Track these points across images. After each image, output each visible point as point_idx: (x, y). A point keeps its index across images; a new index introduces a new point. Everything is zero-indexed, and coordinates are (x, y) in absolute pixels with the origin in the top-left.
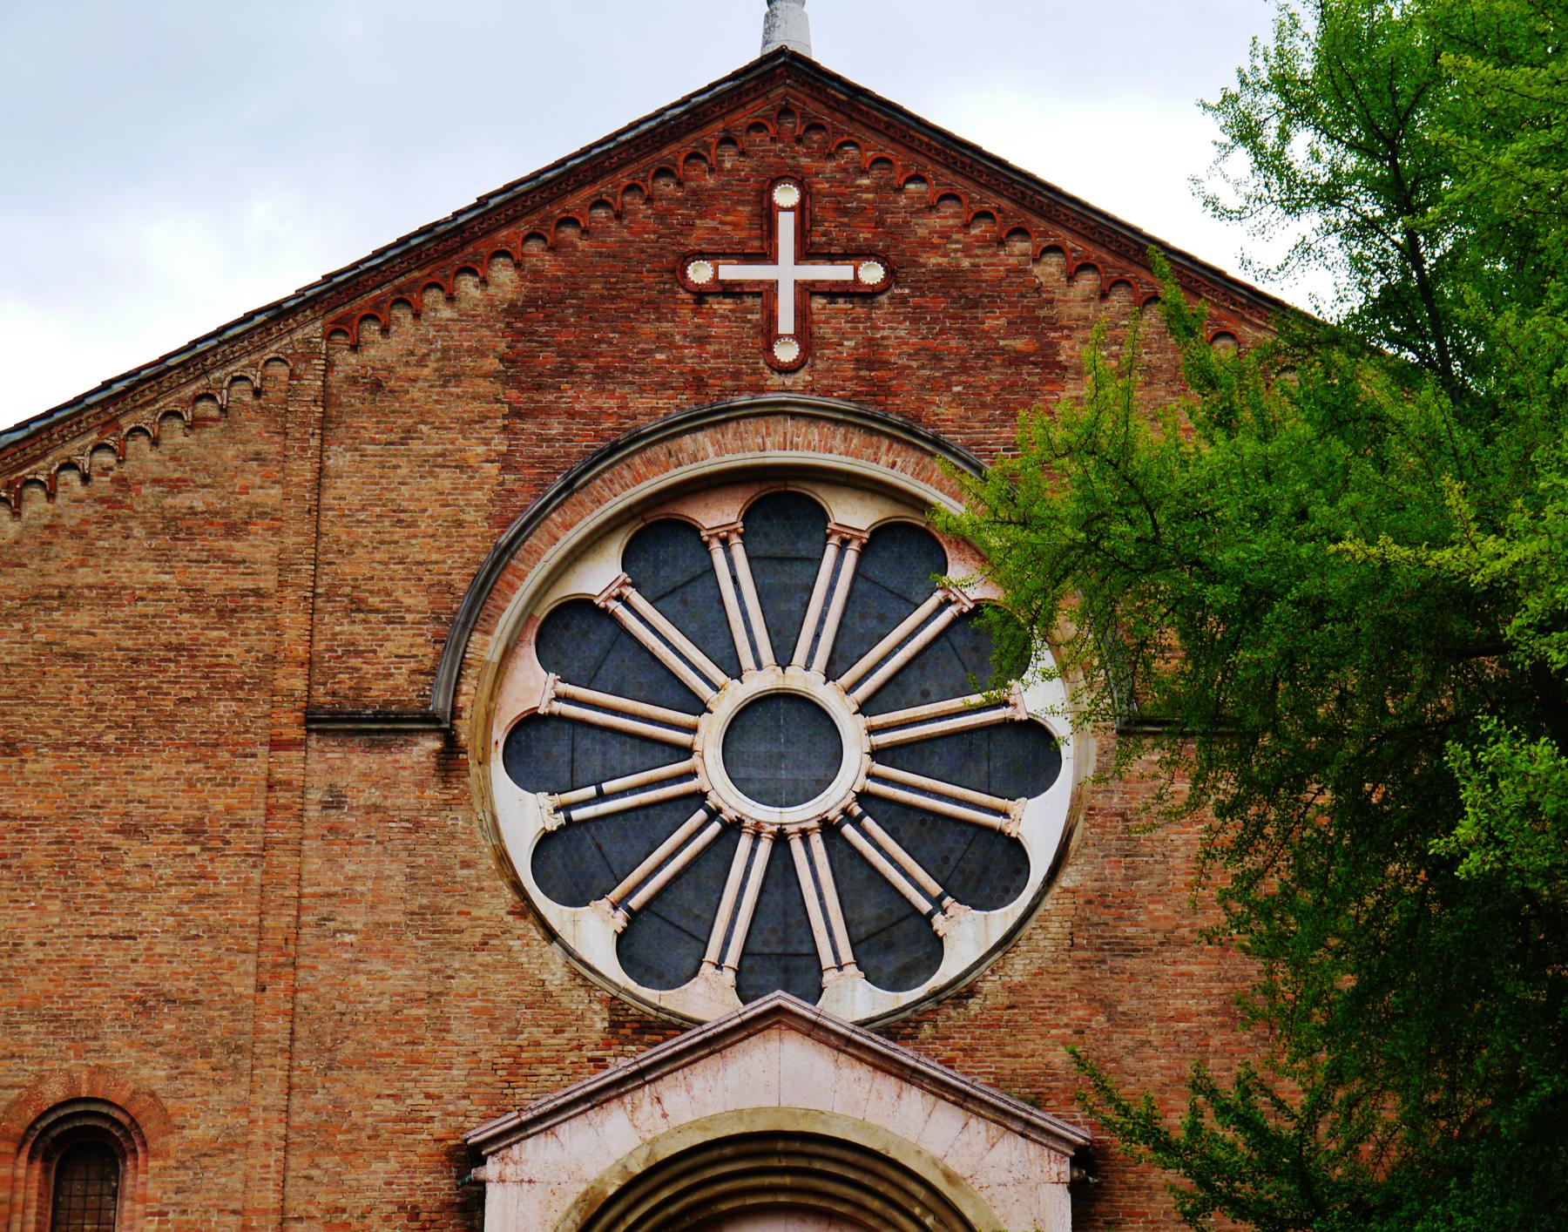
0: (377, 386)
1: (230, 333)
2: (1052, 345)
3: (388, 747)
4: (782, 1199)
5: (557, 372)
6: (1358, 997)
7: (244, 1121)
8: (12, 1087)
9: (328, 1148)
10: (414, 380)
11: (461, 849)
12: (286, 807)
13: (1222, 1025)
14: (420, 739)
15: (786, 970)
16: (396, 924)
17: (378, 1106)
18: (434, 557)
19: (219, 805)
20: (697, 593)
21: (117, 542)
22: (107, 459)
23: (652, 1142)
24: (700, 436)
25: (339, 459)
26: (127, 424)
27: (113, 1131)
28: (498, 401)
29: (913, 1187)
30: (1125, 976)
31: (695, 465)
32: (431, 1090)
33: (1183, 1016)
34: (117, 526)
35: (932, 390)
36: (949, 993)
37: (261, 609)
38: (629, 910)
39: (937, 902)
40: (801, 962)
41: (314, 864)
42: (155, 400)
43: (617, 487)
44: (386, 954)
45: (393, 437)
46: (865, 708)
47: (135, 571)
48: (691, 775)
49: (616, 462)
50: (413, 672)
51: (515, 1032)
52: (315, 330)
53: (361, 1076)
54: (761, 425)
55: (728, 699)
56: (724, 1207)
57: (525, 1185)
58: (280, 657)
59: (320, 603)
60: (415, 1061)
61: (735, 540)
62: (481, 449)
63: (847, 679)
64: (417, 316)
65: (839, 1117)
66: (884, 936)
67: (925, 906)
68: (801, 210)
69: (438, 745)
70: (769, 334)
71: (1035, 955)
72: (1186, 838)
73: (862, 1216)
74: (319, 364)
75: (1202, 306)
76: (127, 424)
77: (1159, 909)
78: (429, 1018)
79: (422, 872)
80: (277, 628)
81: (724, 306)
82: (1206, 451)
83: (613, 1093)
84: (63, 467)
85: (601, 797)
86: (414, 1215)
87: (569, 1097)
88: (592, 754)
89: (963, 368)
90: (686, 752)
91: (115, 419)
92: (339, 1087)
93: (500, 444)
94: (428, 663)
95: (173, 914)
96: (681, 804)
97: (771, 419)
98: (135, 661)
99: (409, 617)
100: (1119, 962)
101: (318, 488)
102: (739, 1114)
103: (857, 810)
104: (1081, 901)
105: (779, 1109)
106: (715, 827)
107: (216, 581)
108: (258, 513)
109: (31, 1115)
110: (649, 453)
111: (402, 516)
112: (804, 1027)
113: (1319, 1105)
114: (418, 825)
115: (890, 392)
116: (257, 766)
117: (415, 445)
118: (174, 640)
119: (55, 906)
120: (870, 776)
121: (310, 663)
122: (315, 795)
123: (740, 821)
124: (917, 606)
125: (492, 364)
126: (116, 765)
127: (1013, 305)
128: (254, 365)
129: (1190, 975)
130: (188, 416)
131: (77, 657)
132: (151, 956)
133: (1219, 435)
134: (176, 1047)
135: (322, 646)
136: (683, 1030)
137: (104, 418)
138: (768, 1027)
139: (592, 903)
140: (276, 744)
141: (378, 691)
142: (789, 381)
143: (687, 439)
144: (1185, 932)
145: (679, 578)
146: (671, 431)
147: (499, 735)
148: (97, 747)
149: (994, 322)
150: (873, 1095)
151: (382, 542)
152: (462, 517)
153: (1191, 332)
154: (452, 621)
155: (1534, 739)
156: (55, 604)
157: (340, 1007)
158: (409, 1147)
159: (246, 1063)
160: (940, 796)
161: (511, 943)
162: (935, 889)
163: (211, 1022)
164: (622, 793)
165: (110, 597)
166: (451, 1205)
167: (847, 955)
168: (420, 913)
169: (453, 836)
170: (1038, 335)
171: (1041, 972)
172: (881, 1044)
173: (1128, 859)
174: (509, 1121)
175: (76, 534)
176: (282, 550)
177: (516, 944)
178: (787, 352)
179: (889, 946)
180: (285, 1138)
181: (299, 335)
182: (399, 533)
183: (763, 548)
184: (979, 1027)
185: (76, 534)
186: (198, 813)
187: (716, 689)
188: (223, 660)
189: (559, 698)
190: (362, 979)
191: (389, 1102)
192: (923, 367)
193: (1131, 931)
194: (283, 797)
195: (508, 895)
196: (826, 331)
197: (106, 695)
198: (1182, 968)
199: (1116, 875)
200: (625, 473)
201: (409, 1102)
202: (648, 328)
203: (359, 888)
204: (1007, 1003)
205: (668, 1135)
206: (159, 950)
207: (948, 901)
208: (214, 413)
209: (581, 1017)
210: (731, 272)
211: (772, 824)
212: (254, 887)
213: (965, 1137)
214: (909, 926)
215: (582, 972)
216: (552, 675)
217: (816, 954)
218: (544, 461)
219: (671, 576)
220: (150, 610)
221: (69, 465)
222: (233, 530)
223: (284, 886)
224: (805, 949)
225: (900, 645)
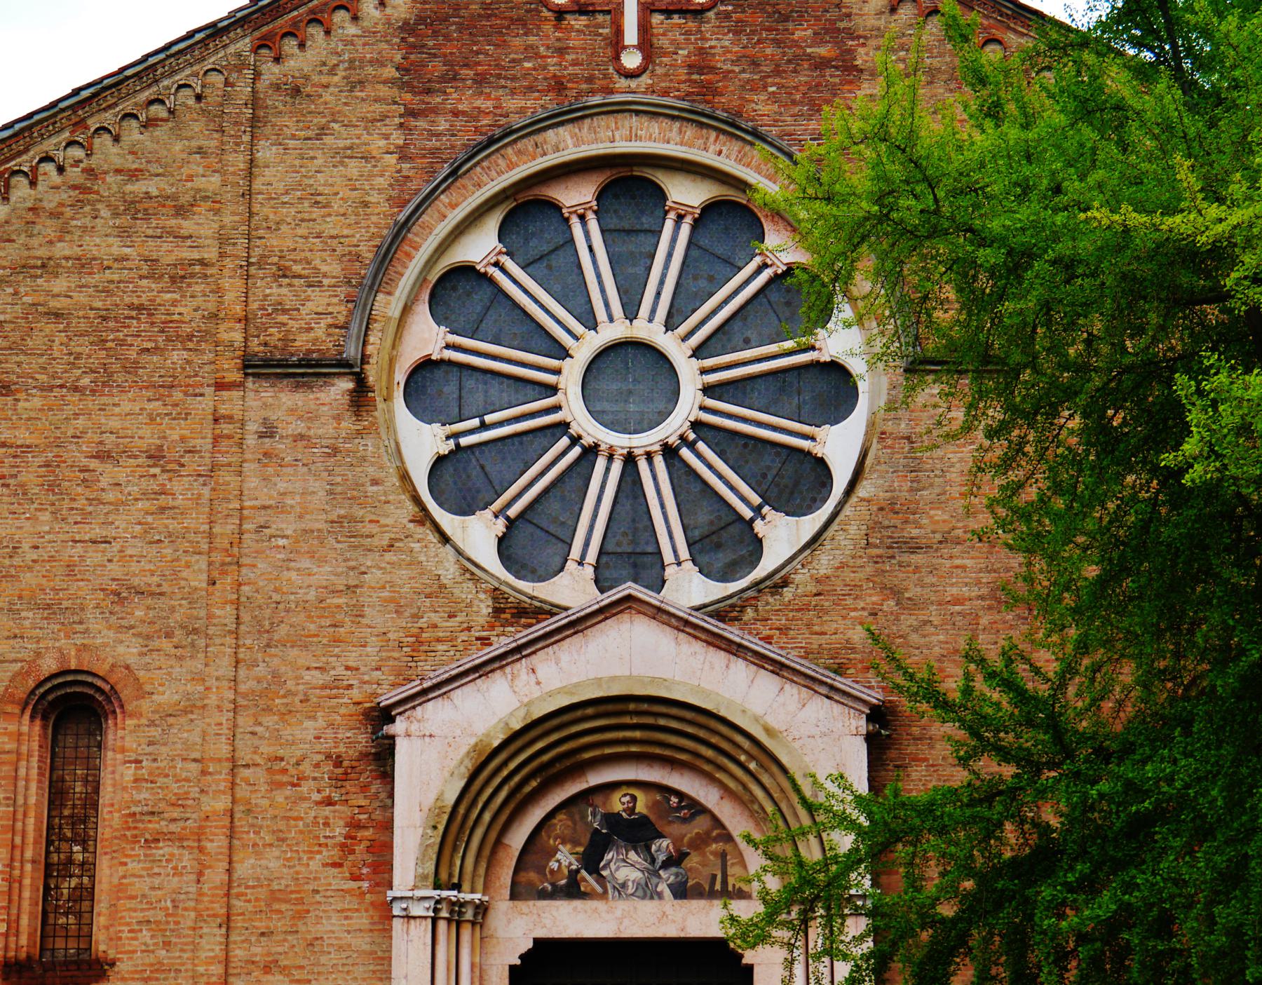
0: (296, 91)
1: (175, 48)
2: (850, 51)
4: (634, 749)
5: (443, 79)
6: (1102, 583)
7: (201, 688)
8: (15, 661)
9: (268, 710)
10: (327, 86)
11: (371, 469)
12: (229, 437)
13: (990, 608)
14: (336, 381)
15: (635, 565)
16: (319, 530)
17: (307, 676)
18: (345, 232)
19: (175, 435)
20: (559, 260)
21: (87, 221)
22: (77, 153)
23: (528, 704)
24: (561, 130)
25: (265, 152)
26: (93, 124)
27: (97, 696)
28: (395, 103)
29: (739, 739)
30: (911, 569)
31: (557, 155)
32: (350, 664)
33: (957, 601)
34: (87, 209)
35: (751, 90)
36: (768, 583)
37: (206, 276)
38: (508, 518)
39: (757, 510)
40: (648, 560)
41: (252, 482)
42: (115, 105)
43: (493, 174)
44: (312, 554)
45: (310, 133)
46: (697, 353)
47: (105, 245)
48: (557, 408)
49: (493, 153)
50: (330, 326)
51: (417, 616)
52: (244, 45)
53: (295, 652)
54: (611, 120)
55: (585, 347)
56: (587, 755)
57: (427, 739)
58: (222, 315)
59: (253, 270)
60: (337, 641)
61: (591, 216)
62: (382, 143)
63: (683, 329)
64: (328, 32)
65: (679, 683)
66: (714, 537)
67: (748, 513)
69: (351, 385)
70: (617, 44)
71: (838, 552)
72: (960, 456)
73: (698, 763)
74: (248, 73)
75: (974, 17)
76: (93, 124)
77: (938, 515)
78: (348, 606)
79: (339, 489)
80: (218, 291)
81: (578, 22)
82: (978, 137)
83: (497, 665)
84: (42, 160)
85: (484, 426)
86: (338, 763)
87: (461, 669)
88: (476, 392)
89: (777, 72)
90: (553, 390)
91: (84, 120)
92: (276, 661)
93: (398, 138)
94: (342, 319)
95: (140, 523)
96: (548, 432)
97: (619, 116)
98: (105, 319)
99: (326, 282)
100: (905, 558)
101: (250, 175)
102: (598, 681)
103: (692, 436)
104: (875, 508)
105: (630, 677)
106: (577, 451)
107: (169, 253)
108: (200, 197)
109: (31, 683)
110: (519, 145)
111: (319, 198)
112: (651, 611)
113: (1069, 671)
114: (335, 451)
115: (716, 92)
116: (205, 404)
117: (328, 140)
118: (136, 301)
119: (46, 516)
120: (703, 408)
121: (246, 319)
122: (252, 427)
123: (597, 445)
124: (740, 269)
125: (390, 72)
126: (91, 403)
127: (818, 19)
128: (196, 75)
129: (963, 567)
130: (143, 118)
131: (57, 315)
132: (123, 557)
133: (989, 124)
134: (145, 629)
135: (255, 306)
136: (553, 614)
137: (74, 119)
138: (621, 612)
139: (478, 513)
140: (220, 386)
141: (302, 343)
142: (633, 84)
143: (550, 133)
144: (959, 532)
145: (545, 248)
146: (537, 126)
147: (400, 377)
148: (76, 389)
149: (803, 33)
150: (707, 667)
151: (303, 220)
152: (368, 199)
153: (965, 39)
154: (361, 284)
155: (1248, 371)
156: (39, 272)
157: (276, 597)
158: (334, 710)
159: (201, 643)
160: (759, 424)
161: (412, 545)
162: (756, 499)
163: (173, 610)
164: (500, 424)
165: (83, 266)
166: (367, 755)
167: (684, 553)
168: (338, 522)
169: (364, 459)
170: (838, 43)
171: (843, 566)
172: (713, 625)
173: (914, 474)
174: (413, 688)
175: (55, 215)
176: (222, 227)
177: (416, 546)
178: (632, 60)
179: (718, 546)
180: (234, 702)
181: (231, 49)
182: (316, 213)
183: (613, 223)
184: (792, 610)
185: (55, 215)
186: (158, 442)
187: (577, 338)
188: (176, 317)
189: (448, 346)
190: (293, 575)
191: (317, 673)
192: (744, 71)
193: (915, 532)
194: (226, 428)
195: (410, 507)
196: (663, 42)
197: (82, 346)
198: (958, 562)
199: (903, 487)
200: (500, 161)
201: (332, 673)
202: (517, 42)
203: (289, 502)
204: (815, 591)
205: (541, 699)
206: (129, 552)
207: (766, 509)
208: (164, 115)
209: (470, 605)
211: (623, 448)
212: (205, 501)
213: (781, 699)
214: (735, 530)
215: (470, 568)
216: (443, 328)
217: (659, 553)
218: (434, 152)
219: (537, 246)
220: (116, 277)
221: (47, 159)
223: (228, 500)
224: (650, 549)
225: (726, 301)
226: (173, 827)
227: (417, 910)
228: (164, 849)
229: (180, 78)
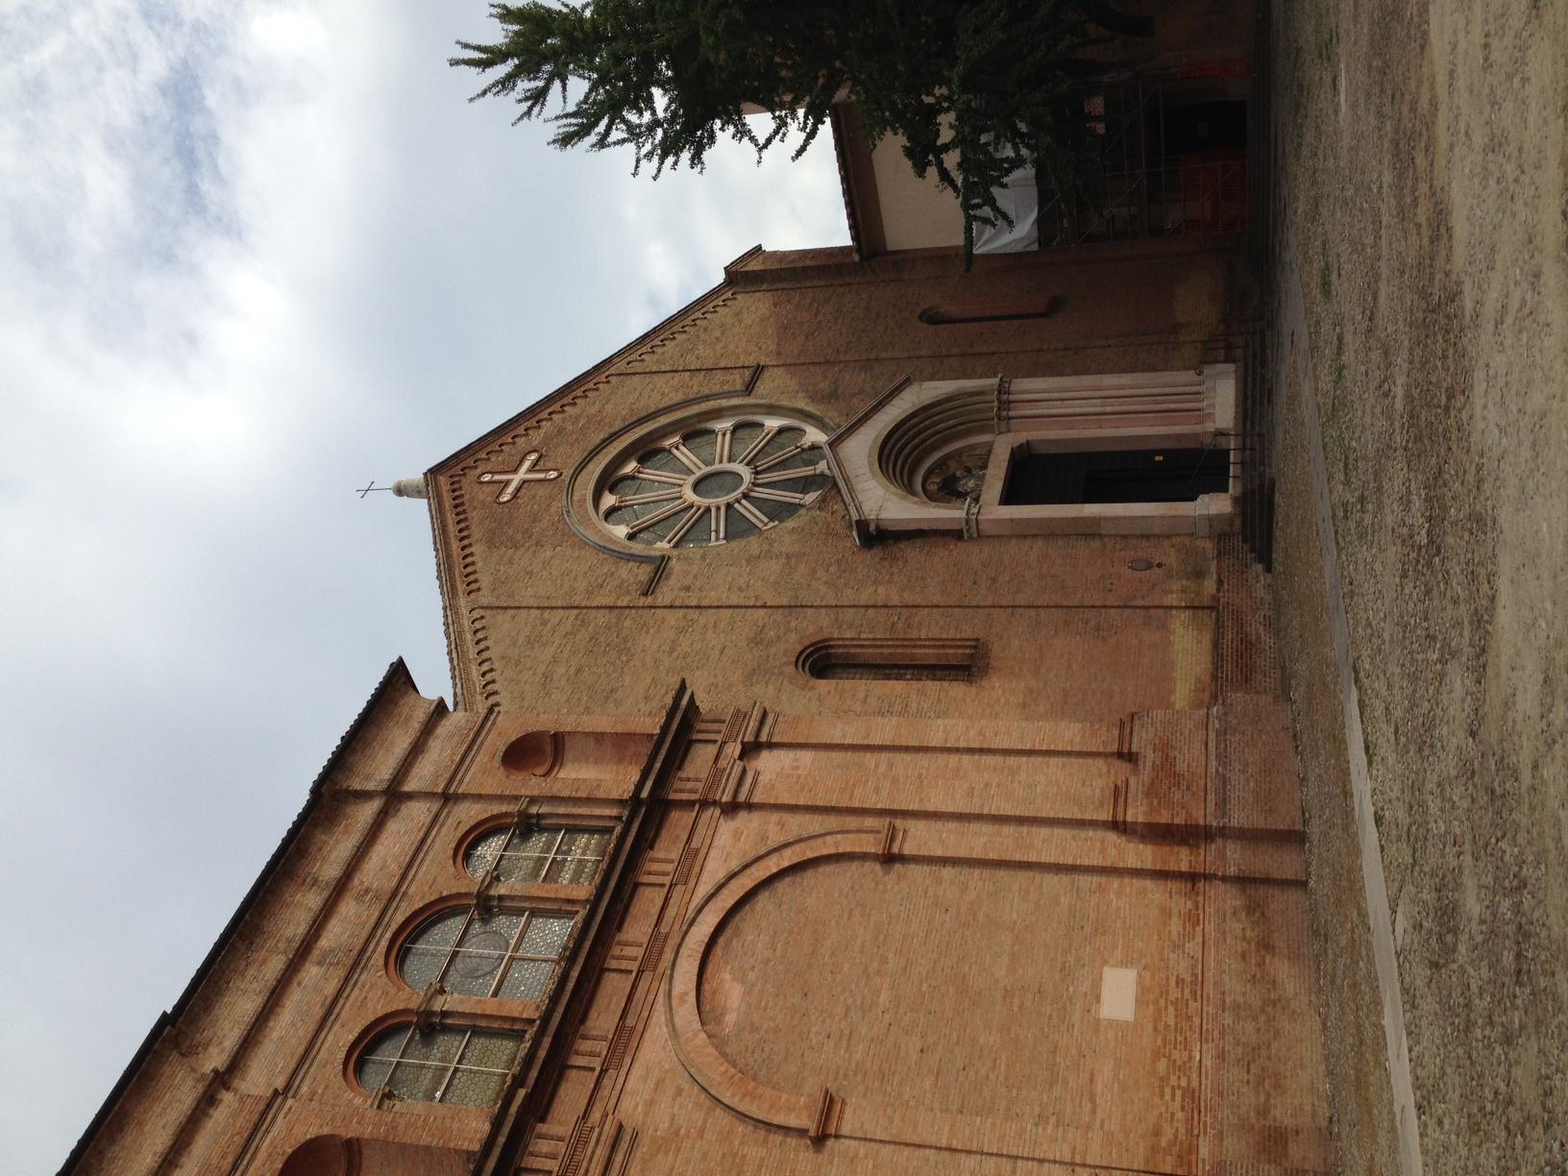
3: (670, 574)
14: (669, 566)
25: (530, 591)
55: (690, 496)
63: (695, 470)
68: (493, 473)
81: (523, 491)
85: (717, 531)
106: (744, 502)
107: (568, 626)
114: (710, 565)
131: (579, 671)
182: (573, 574)
210: (511, 489)
217: (806, 477)
221: (483, 675)
227: (975, 510)
229: (466, 623)
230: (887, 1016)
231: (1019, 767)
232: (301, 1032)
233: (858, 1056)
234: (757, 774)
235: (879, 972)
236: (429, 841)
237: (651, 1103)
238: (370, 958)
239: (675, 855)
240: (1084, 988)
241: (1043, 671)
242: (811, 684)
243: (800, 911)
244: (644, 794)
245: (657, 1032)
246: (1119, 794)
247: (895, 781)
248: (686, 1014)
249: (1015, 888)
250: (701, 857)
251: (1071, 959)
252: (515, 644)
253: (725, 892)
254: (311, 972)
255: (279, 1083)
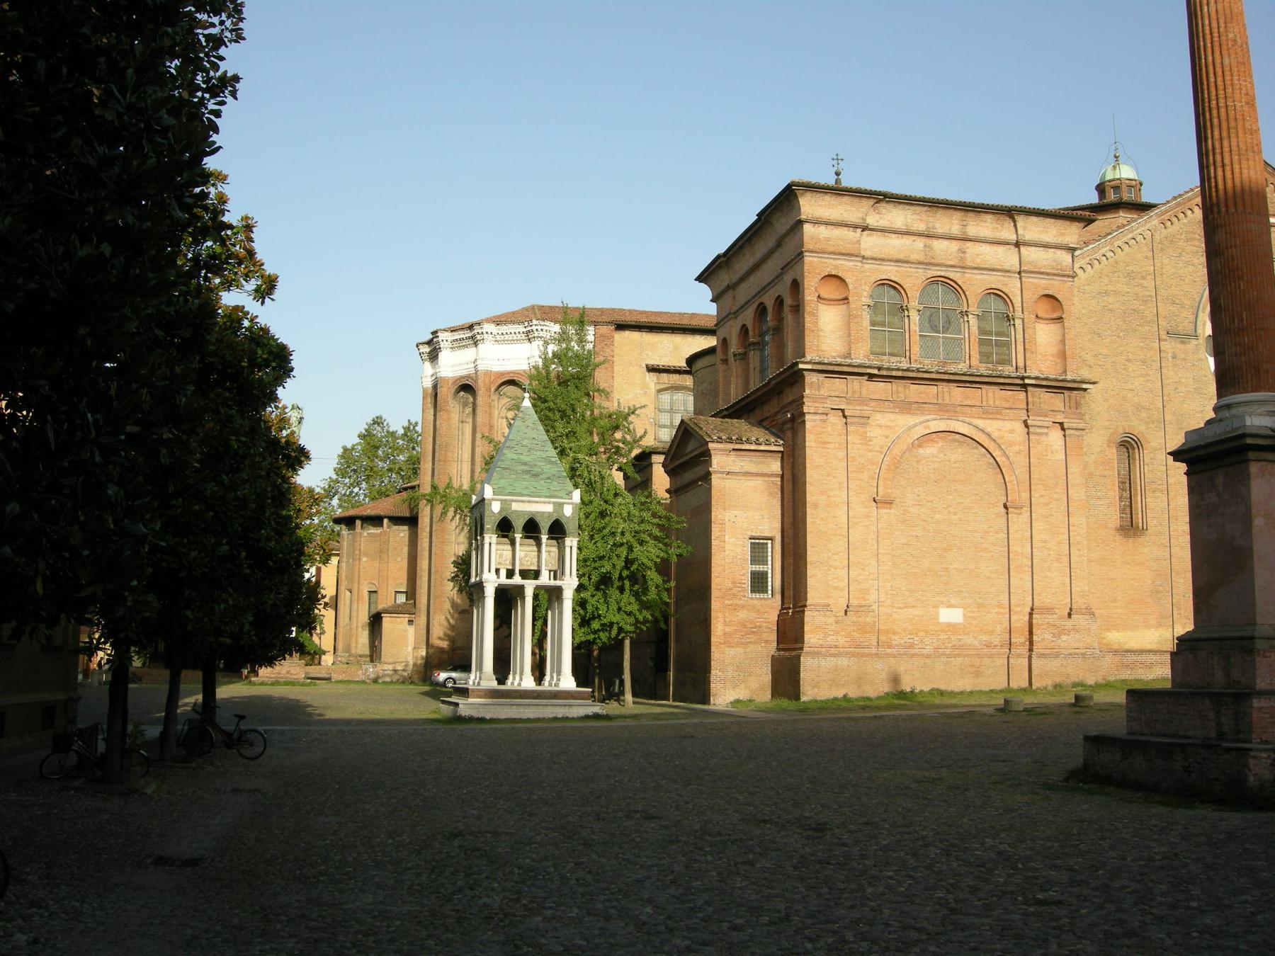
25: (1166, 261)
64: (1179, 220)
114: (1194, 365)
119: (1114, 380)
190: (1185, 406)
222: (1143, 278)
226: (1160, 487)
228: (1157, 494)
230: (930, 519)
231: (1061, 563)
232: (892, 253)
233: (911, 509)
234: (1047, 434)
235: (949, 512)
236: (994, 273)
237: (880, 426)
238: (929, 269)
239: (998, 403)
240: (953, 601)
241: (1128, 566)
242: (1112, 444)
243: (975, 470)
244: (1027, 381)
245: (910, 420)
246: (1050, 610)
247: (1047, 504)
248: (920, 431)
249: (998, 567)
250: (998, 416)
251: (965, 594)
252: (1127, 266)
253: (980, 434)
254: (920, 243)
255: (867, 253)
